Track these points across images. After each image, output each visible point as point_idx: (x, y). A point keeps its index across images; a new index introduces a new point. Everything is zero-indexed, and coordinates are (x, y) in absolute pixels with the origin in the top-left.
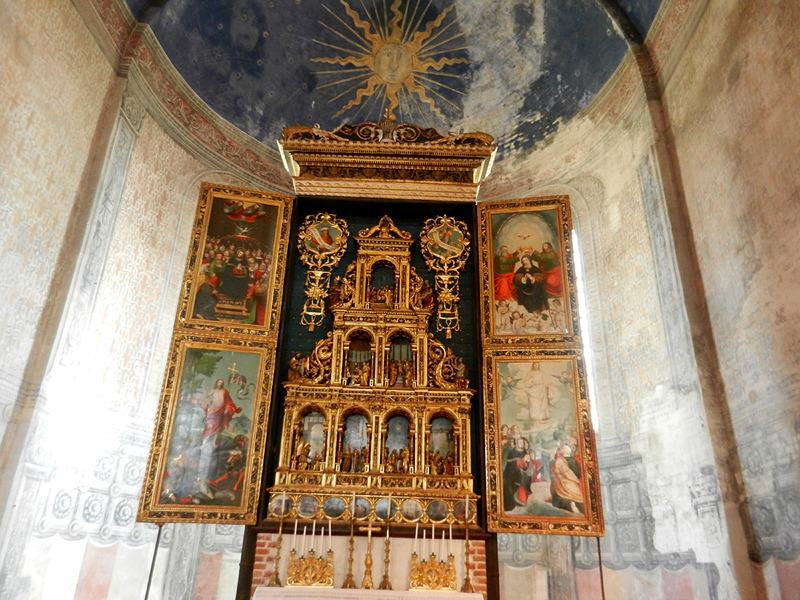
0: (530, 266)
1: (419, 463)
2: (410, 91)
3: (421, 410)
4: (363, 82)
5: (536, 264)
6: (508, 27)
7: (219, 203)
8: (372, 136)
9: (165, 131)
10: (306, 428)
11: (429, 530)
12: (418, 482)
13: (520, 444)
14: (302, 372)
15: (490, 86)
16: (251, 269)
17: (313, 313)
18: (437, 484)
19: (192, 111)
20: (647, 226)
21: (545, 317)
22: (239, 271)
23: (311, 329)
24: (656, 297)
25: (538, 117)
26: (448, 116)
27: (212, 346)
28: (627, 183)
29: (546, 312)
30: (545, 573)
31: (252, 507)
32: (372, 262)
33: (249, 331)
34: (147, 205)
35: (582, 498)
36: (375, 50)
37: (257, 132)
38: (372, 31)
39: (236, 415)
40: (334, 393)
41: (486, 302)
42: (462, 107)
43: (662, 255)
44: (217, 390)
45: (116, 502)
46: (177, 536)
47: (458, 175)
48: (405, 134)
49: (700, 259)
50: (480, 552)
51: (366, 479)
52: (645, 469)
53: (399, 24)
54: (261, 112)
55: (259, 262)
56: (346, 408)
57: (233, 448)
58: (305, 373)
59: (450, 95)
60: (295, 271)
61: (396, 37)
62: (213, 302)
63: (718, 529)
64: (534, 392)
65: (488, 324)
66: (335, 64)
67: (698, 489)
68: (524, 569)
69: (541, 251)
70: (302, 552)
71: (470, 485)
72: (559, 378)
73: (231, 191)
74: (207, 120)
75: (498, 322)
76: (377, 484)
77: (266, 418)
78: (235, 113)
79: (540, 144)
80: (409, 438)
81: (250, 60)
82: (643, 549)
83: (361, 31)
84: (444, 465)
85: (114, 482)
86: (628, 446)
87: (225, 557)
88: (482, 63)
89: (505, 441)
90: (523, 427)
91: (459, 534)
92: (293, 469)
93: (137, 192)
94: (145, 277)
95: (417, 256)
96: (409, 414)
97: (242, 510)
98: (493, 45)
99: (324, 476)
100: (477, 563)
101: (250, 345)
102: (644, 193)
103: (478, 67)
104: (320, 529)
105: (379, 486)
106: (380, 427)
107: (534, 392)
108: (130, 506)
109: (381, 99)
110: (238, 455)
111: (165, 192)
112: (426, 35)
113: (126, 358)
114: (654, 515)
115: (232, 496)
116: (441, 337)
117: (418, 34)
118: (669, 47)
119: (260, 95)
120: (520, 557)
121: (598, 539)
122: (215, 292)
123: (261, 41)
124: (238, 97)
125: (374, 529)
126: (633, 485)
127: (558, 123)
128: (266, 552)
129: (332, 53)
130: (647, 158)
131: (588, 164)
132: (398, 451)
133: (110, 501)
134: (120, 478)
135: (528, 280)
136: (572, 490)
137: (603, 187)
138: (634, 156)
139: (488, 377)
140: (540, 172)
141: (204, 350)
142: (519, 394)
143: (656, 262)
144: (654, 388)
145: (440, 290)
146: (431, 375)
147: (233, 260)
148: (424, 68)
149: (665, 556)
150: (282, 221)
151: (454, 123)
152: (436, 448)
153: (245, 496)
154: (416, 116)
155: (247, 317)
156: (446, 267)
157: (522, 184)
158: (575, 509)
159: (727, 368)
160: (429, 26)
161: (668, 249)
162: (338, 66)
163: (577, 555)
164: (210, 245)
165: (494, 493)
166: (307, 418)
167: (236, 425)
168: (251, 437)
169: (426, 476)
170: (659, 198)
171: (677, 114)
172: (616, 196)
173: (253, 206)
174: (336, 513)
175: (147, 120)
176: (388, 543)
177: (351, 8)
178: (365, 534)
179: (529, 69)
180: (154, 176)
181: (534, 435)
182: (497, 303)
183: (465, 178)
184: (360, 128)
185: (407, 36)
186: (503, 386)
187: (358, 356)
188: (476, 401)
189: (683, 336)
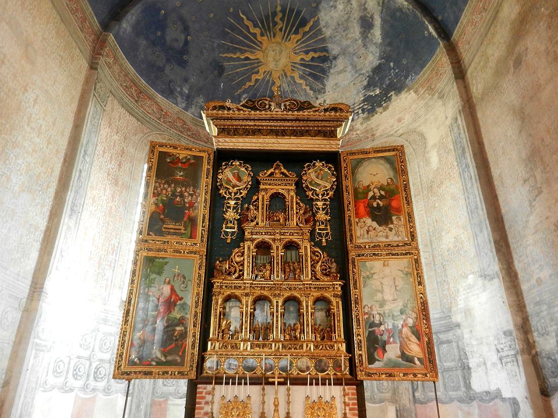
0: (379, 195)
2: (288, 75)
3: (307, 296)
4: (256, 70)
5: (383, 193)
6: (356, 30)
7: (162, 155)
8: (267, 107)
9: (123, 106)
10: (227, 310)
11: (317, 380)
12: (307, 346)
14: (224, 271)
17: (229, 230)
18: (321, 347)
19: (140, 92)
20: (458, 165)
21: (391, 230)
22: (178, 201)
23: (229, 241)
24: (466, 214)
25: (378, 91)
27: (162, 254)
28: (442, 136)
29: (391, 226)
30: (394, 408)
31: (192, 366)
32: (269, 194)
33: (187, 243)
34: (111, 157)
35: (421, 354)
37: (184, 105)
38: (262, 35)
39: (179, 302)
40: (247, 285)
41: (349, 220)
42: (324, 85)
43: (469, 185)
44: (166, 285)
45: (94, 365)
47: (326, 132)
48: (289, 105)
49: (496, 187)
50: (353, 394)
51: (271, 345)
52: (462, 333)
53: (281, 30)
54: (187, 92)
55: (192, 195)
56: (256, 295)
57: (178, 325)
58: (226, 272)
60: (217, 201)
61: (278, 38)
62: (160, 223)
63: (518, 374)
64: (385, 281)
65: (351, 235)
66: (237, 58)
67: (502, 346)
68: (378, 405)
70: (229, 397)
71: (343, 347)
72: (402, 271)
73: (170, 147)
74: (151, 98)
75: (358, 234)
76: (279, 348)
77: (200, 304)
78: (169, 93)
79: (380, 110)
80: (299, 316)
81: (179, 56)
82: (463, 389)
83: (254, 35)
84: (325, 333)
85: (93, 351)
87: (169, 402)
88: (338, 55)
89: (366, 316)
90: (378, 306)
91: (338, 382)
92: (220, 339)
93: (105, 148)
94: (111, 208)
95: (300, 188)
96: (299, 299)
97: (186, 369)
98: (345, 43)
99: (242, 344)
100: (351, 402)
101: (188, 253)
102: (455, 143)
103: (335, 58)
104: (240, 381)
105: (280, 350)
106: (279, 308)
107: (385, 281)
108: (104, 368)
109: (268, 81)
110: (182, 330)
111: (123, 148)
112: (299, 37)
113: (100, 264)
114: (471, 365)
116: (318, 244)
117: (293, 36)
118: (469, 43)
119: (186, 80)
120: (376, 396)
121: (434, 383)
122: (162, 216)
123: (186, 42)
124: (170, 82)
125: (279, 380)
126: (454, 344)
127: (392, 95)
128: (203, 398)
129: (234, 50)
130: (456, 119)
131: (414, 124)
132: (292, 325)
133: (90, 365)
134: (97, 349)
135: (378, 204)
136: (415, 349)
137: (425, 139)
138: (447, 118)
139: (353, 271)
140: (381, 129)
141: (155, 257)
142: (374, 283)
143: (465, 190)
144: (467, 277)
145: (317, 212)
146: (313, 271)
147: (174, 194)
148: (298, 59)
149: (479, 393)
150: (206, 166)
151: (319, 96)
152: (318, 322)
153: (188, 358)
154: (293, 92)
156: (320, 196)
158: (417, 362)
159: (519, 262)
160: (301, 31)
161: (474, 181)
162: (239, 59)
163: (416, 394)
164: (157, 184)
165: (361, 352)
166: (228, 303)
167: (180, 309)
168: (190, 318)
169: (313, 342)
170: (466, 146)
171: (477, 87)
172: (435, 145)
173: (186, 157)
174: (251, 369)
175: (110, 99)
176: (288, 390)
177: (248, 19)
178: (273, 383)
179: (371, 59)
180: (115, 137)
181: (387, 312)
182: (357, 220)
183: (332, 135)
184: (258, 102)
185: (286, 38)
186: (363, 278)
187: (261, 260)
188: (346, 289)
189: (487, 240)
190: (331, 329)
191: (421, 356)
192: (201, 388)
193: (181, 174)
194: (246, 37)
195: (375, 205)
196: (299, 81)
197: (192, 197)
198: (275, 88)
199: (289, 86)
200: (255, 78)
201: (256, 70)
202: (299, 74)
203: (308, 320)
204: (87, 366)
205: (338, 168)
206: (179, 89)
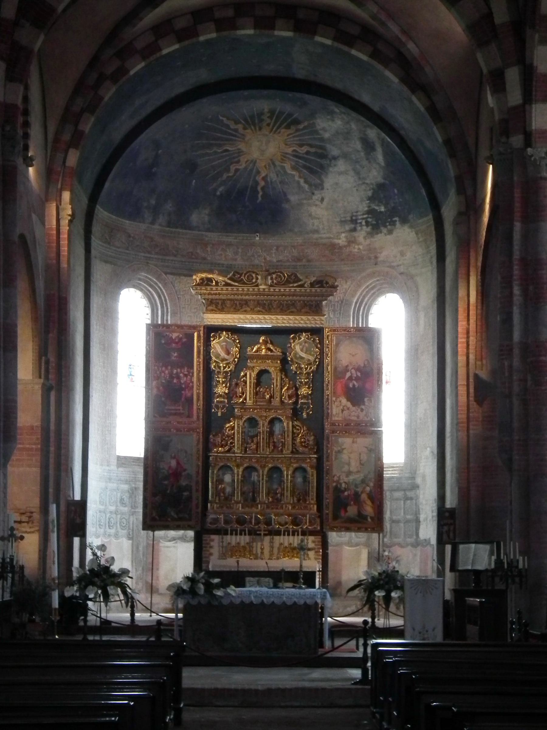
1: (287, 496)
2: (277, 164)
4: (236, 160)
5: (359, 374)
6: (358, 146)
12: (286, 507)
13: (343, 485)
15: (345, 173)
16: (182, 382)
18: (297, 507)
21: (362, 410)
23: (219, 414)
25: (383, 209)
26: (310, 185)
29: (363, 407)
30: (367, 550)
36: (246, 139)
37: (150, 219)
38: (245, 128)
41: (328, 399)
45: (108, 516)
46: (135, 534)
50: (319, 542)
55: (186, 375)
56: (245, 465)
59: (312, 171)
61: (266, 131)
65: (328, 413)
68: (354, 548)
69: (362, 365)
75: (334, 412)
78: (135, 214)
79: (384, 230)
82: (415, 537)
84: (301, 497)
86: (414, 478)
87: (161, 545)
88: (338, 157)
89: (334, 484)
92: (217, 501)
101: (187, 431)
103: (335, 158)
109: (251, 170)
112: (289, 131)
115: (187, 516)
117: (283, 130)
126: (414, 501)
135: (354, 385)
136: (369, 510)
139: (327, 447)
142: (345, 457)
147: (171, 376)
148: (290, 150)
151: (316, 192)
155: (183, 413)
157: (370, 258)
158: (369, 520)
160: (293, 128)
164: (156, 368)
168: (193, 484)
177: (228, 119)
178: (260, 535)
179: (375, 175)
181: (351, 481)
182: (334, 399)
184: (245, 274)
188: (320, 460)
190: (306, 493)
191: (373, 515)
192: (205, 537)
193: (176, 355)
194: (226, 133)
195: (351, 386)
196: (289, 171)
197: (187, 377)
198: (259, 178)
199: (277, 175)
200: (234, 168)
201: (236, 160)
202: (291, 164)
203: (288, 484)
204: (104, 517)
205: (321, 342)
206: (145, 204)
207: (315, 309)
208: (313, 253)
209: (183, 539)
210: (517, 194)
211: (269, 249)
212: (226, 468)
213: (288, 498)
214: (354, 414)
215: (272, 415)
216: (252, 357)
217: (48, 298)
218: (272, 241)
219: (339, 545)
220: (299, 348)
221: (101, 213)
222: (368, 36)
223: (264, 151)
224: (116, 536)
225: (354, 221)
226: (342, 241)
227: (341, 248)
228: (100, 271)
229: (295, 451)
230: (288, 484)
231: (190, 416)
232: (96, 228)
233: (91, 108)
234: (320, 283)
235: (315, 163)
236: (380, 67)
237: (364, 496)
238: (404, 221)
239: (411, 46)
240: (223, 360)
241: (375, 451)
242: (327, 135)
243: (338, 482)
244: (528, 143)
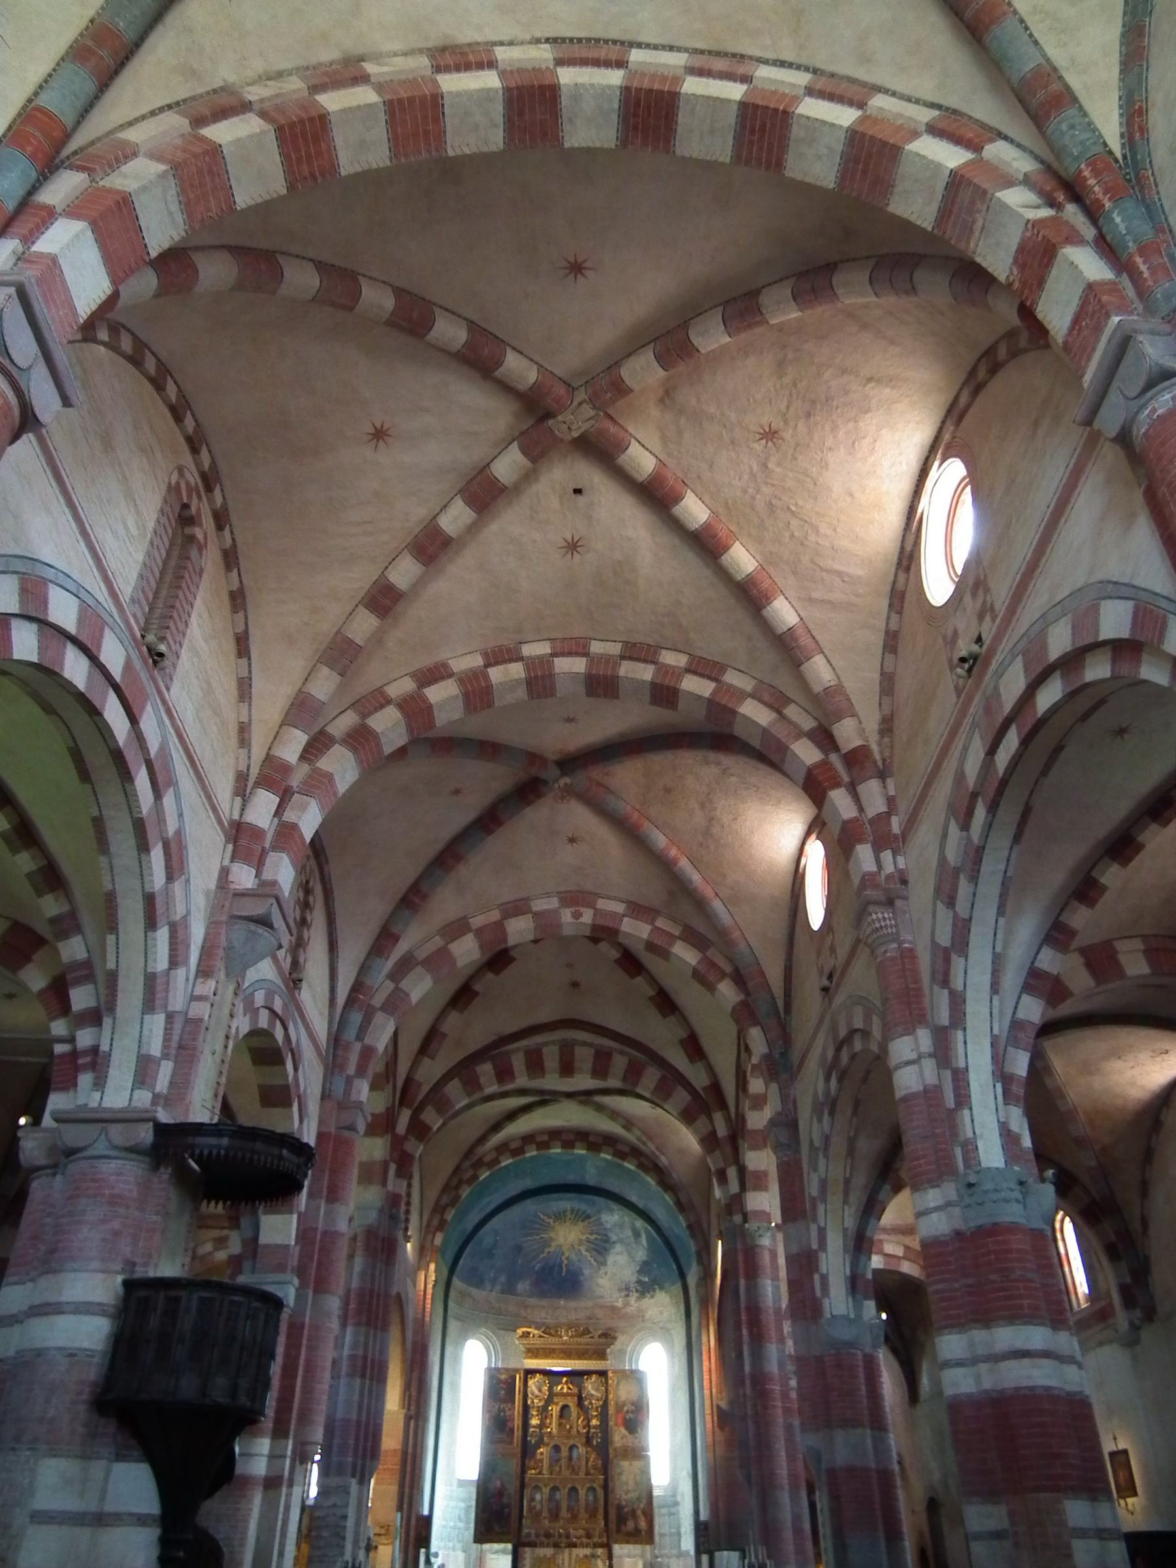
3: (583, 1486)
6: (629, 1233)
15: (621, 1253)
78: (479, 1283)
84: (592, 1514)
86: (674, 1496)
123: (496, 1241)
136: (643, 1524)
142: (624, 1478)
147: (500, 1410)
148: (584, 1237)
154: (579, 1261)
179: (641, 1254)
188: (606, 1480)
196: (584, 1252)
198: (563, 1258)
203: (582, 1502)
205: (607, 1382)
207: (601, 1355)
208: (600, 1313)
209: (504, 1552)
210: (740, 1258)
211: (569, 1310)
212: (537, 1488)
213: (583, 1515)
214: (630, 1440)
215: (571, 1442)
216: (557, 1395)
217: (415, 1344)
218: (572, 1304)
219: (620, 1557)
220: (591, 1386)
221: (456, 1282)
222: (635, 1153)
223: (567, 1238)
224: (454, 1549)
225: (627, 1289)
226: (619, 1304)
227: (619, 1309)
228: (453, 1325)
229: (587, 1474)
230: (582, 1502)
231: (511, 1443)
232: (452, 1294)
233: (454, 1202)
234: (604, 1335)
235: (601, 1247)
236: (643, 1174)
237: (639, 1513)
238: (661, 1288)
239: (663, 1158)
240: (537, 1397)
241: (645, 1472)
242: (609, 1226)
243: (619, 1500)
244: (745, 1220)
